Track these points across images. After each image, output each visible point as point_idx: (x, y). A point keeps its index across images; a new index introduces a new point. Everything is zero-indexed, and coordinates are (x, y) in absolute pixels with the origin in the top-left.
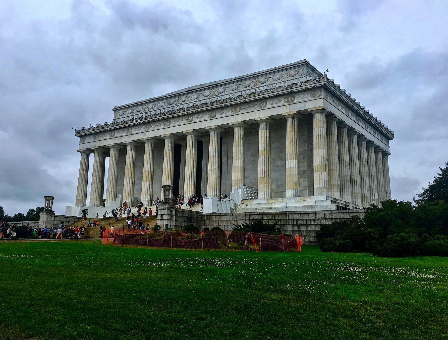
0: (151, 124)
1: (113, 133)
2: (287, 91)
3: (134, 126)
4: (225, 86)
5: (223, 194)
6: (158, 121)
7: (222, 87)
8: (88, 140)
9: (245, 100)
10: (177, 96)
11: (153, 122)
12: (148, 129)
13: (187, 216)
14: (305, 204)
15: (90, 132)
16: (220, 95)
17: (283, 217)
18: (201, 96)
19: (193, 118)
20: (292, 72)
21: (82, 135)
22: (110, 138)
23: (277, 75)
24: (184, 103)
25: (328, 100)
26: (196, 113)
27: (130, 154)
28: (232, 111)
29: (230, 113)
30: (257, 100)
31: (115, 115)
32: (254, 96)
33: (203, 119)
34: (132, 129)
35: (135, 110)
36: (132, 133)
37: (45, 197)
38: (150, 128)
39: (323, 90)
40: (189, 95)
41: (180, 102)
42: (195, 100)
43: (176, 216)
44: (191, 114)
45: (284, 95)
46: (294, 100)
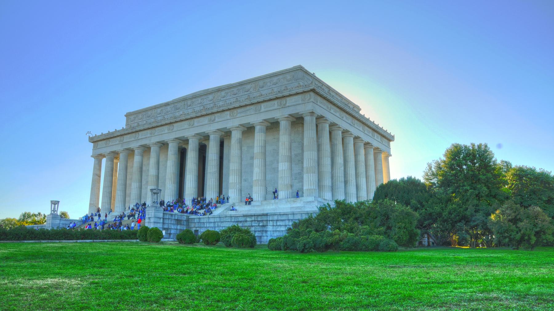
0: (157, 129)
2: (280, 95)
4: (227, 91)
13: (176, 218)
14: (294, 205)
15: (101, 138)
16: (222, 99)
17: (265, 218)
20: (288, 77)
21: (95, 141)
23: (275, 79)
25: (318, 103)
29: (228, 117)
30: (253, 104)
37: (52, 201)
39: (312, 94)
40: (194, 100)
41: (186, 107)
43: (163, 219)
45: (277, 98)
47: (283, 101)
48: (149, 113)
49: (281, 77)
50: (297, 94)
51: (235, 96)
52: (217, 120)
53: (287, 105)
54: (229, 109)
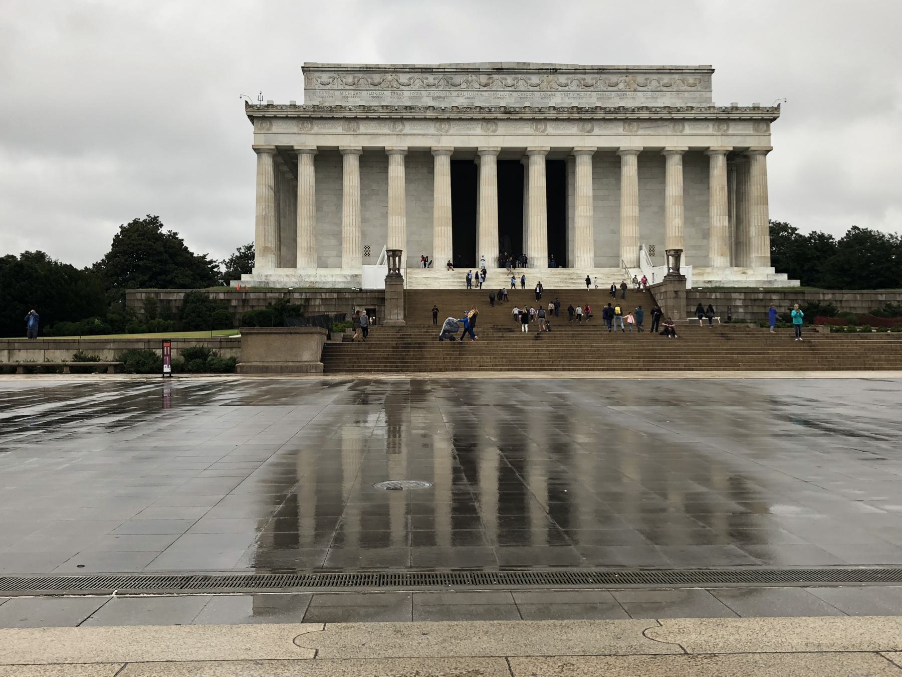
0: (452, 123)
1: (353, 125)
2: (724, 116)
3: (414, 119)
4: (570, 76)
5: (558, 255)
6: (472, 119)
7: (565, 77)
8: (277, 127)
9: (653, 116)
10: (468, 72)
11: (460, 119)
12: (447, 131)
16: (560, 89)
18: (521, 83)
19: (546, 126)
20: (691, 79)
22: (344, 132)
23: (666, 79)
24: (485, 89)
26: (557, 119)
27: (397, 170)
28: (624, 128)
29: (620, 130)
30: (672, 120)
31: (308, 80)
32: (670, 113)
33: (568, 132)
34: (403, 124)
35: (362, 81)
36: (405, 132)
38: (449, 129)
40: (495, 76)
42: (510, 89)
44: (546, 119)
45: (717, 120)
46: (727, 129)
47: (724, 127)
48: (377, 78)
49: (676, 77)
50: (751, 120)
51: (588, 89)
52: (597, 131)
53: (731, 132)
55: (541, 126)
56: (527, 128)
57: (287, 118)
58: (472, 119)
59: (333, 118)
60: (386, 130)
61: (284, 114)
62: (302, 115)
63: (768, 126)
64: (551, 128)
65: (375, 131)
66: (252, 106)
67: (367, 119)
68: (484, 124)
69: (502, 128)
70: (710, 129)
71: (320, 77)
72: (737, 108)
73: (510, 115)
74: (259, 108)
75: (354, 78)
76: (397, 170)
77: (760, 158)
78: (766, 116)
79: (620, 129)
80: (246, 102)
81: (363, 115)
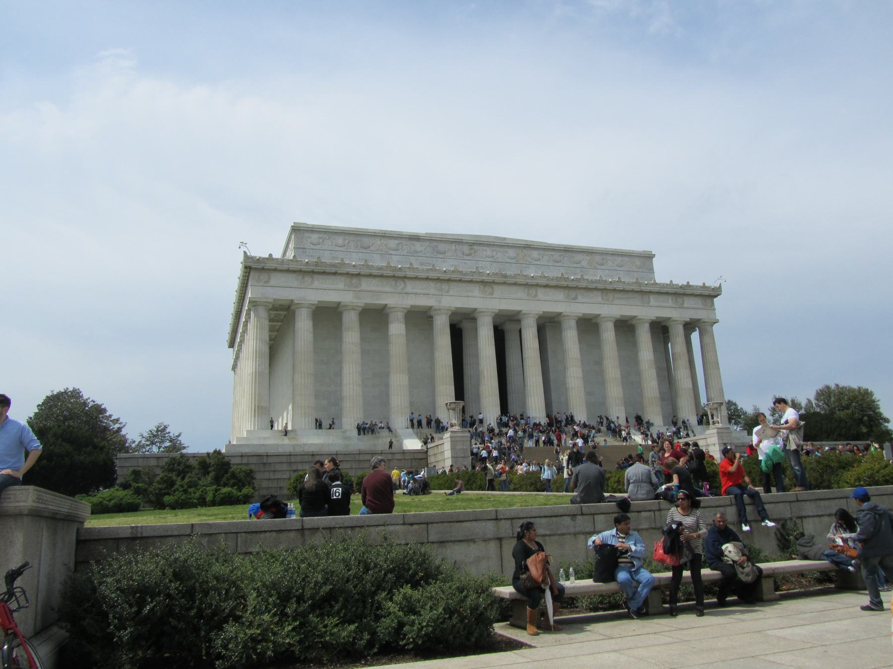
0: (452, 284)
1: (355, 280)
2: (682, 291)
3: (416, 278)
6: (471, 281)
9: (627, 288)
12: (448, 291)
16: (534, 262)
18: (499, 255)
20: (638, 262)
23: (619, 260)
24: (468, 258)
26: (547, 286)
27: (397, 329)
29: (600, 299)
40: (475, 247)
44: (537, 285)
47: (680, 300)
48: (366, 241)
49: (626, 259)
52: (580, 298)
53: (685, 305)
54: (604, 291)
55: (532, 291)
56: (521, 293)
57: (288, 271)
58: (471, 281)
59: (335, 274)
60: (387, 289)
61: (285, 267)
62: (304, 268)
63: (713, 302)
64: (541, 293)
65: (376, 289)
66: (252, 258)
67: (370, 276)
68: (482, 287)
69: (498, 291)
70: (670, 301)
71: (310, 238)
72: (690, 286)
73: (506, 282)
74: (260, 260)
75: (344, 240)
76: (397, 329)
77: (709, 328)
78: (712, 293)
79: (598, 297)
80: (245, 252)
81: (366, 271)
